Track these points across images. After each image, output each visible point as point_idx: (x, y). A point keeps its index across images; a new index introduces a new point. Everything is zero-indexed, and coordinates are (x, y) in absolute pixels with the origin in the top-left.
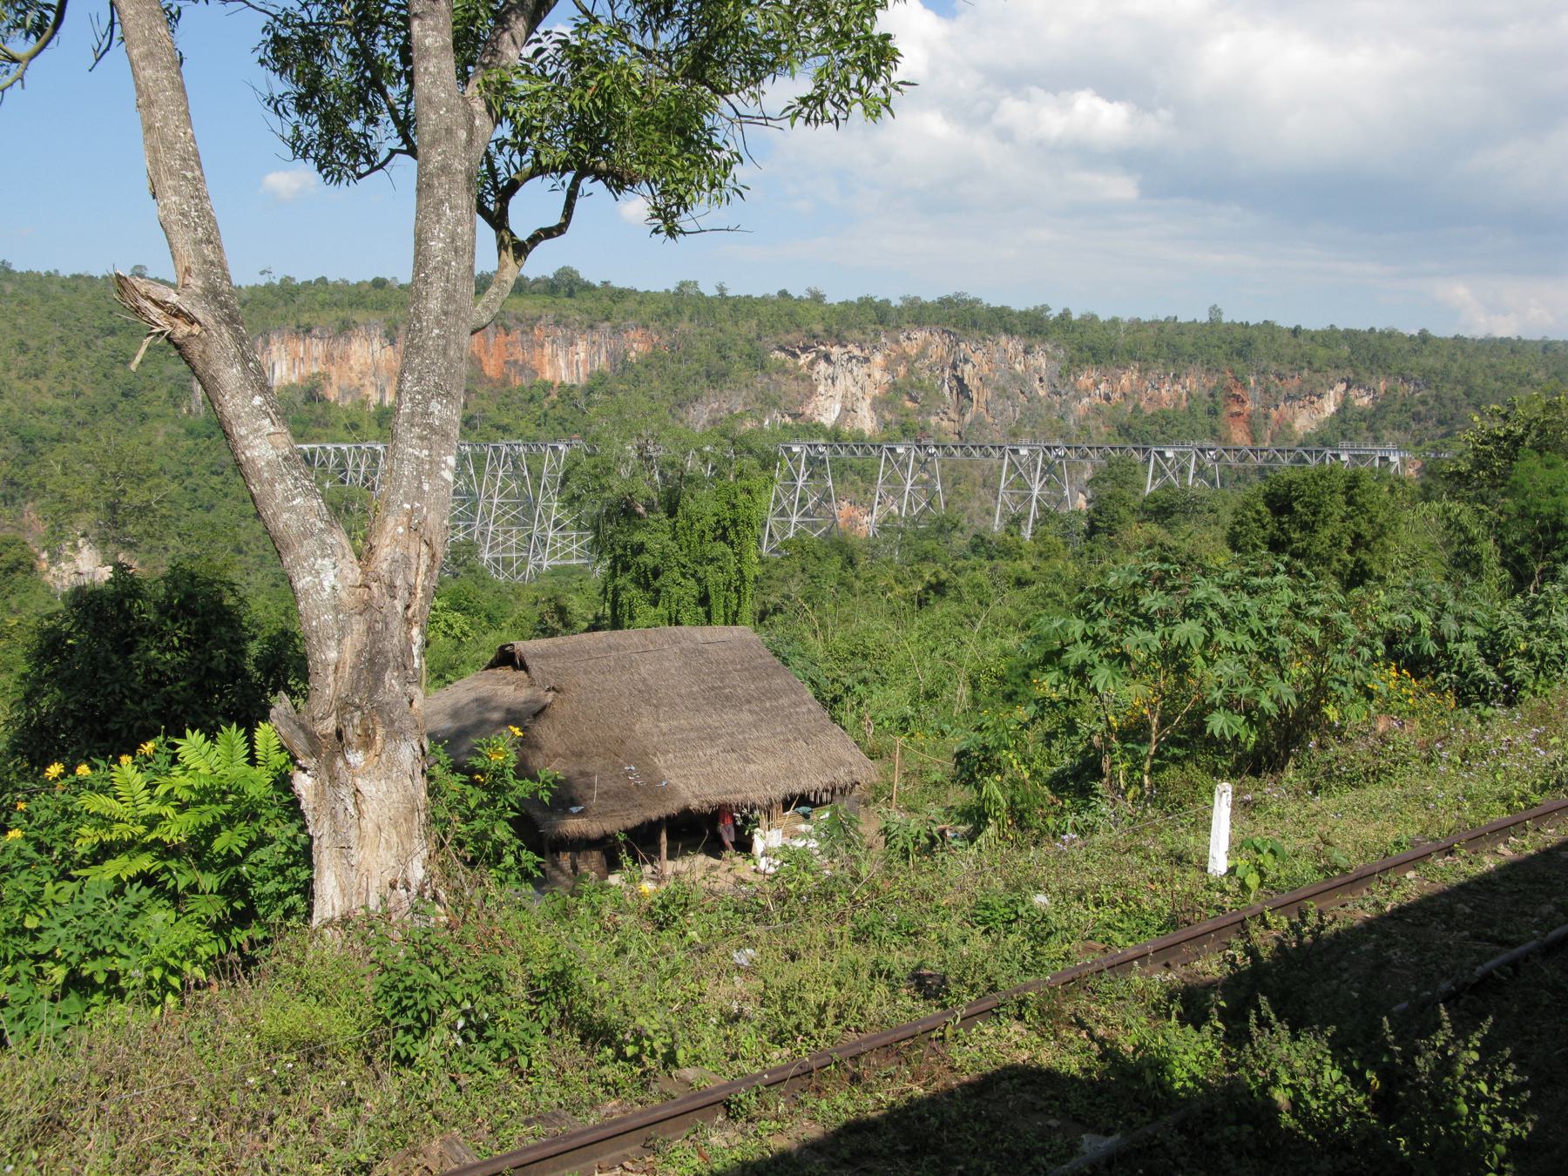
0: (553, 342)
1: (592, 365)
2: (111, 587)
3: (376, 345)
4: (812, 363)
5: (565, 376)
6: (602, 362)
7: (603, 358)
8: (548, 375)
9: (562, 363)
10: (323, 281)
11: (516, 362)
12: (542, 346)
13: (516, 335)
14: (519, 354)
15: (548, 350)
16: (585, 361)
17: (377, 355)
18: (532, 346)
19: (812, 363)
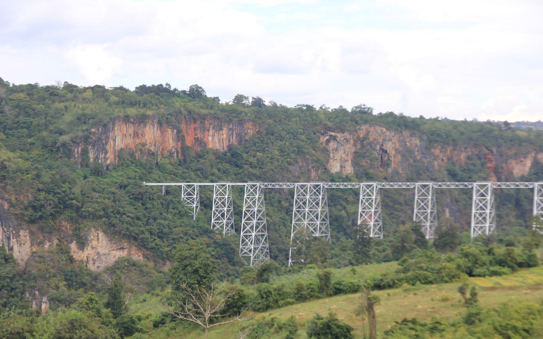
0: (214, 128)
1: (229, 141)
2: (360, 308)
3: (156, 128)
4: (328, 141)
5: (217, 146)
6: (234, 141)
7: (234, 138)
8: (210, 146)
9: (217, 141)
10: (391, 114)
11: (198, 138)
12: (209, 130)
13: (198, 124)
14: (199, 136)
15: (211, 132)
16: (226, 138)
17: (155, 133)
18: (204, 130)
19: (328, 141)
